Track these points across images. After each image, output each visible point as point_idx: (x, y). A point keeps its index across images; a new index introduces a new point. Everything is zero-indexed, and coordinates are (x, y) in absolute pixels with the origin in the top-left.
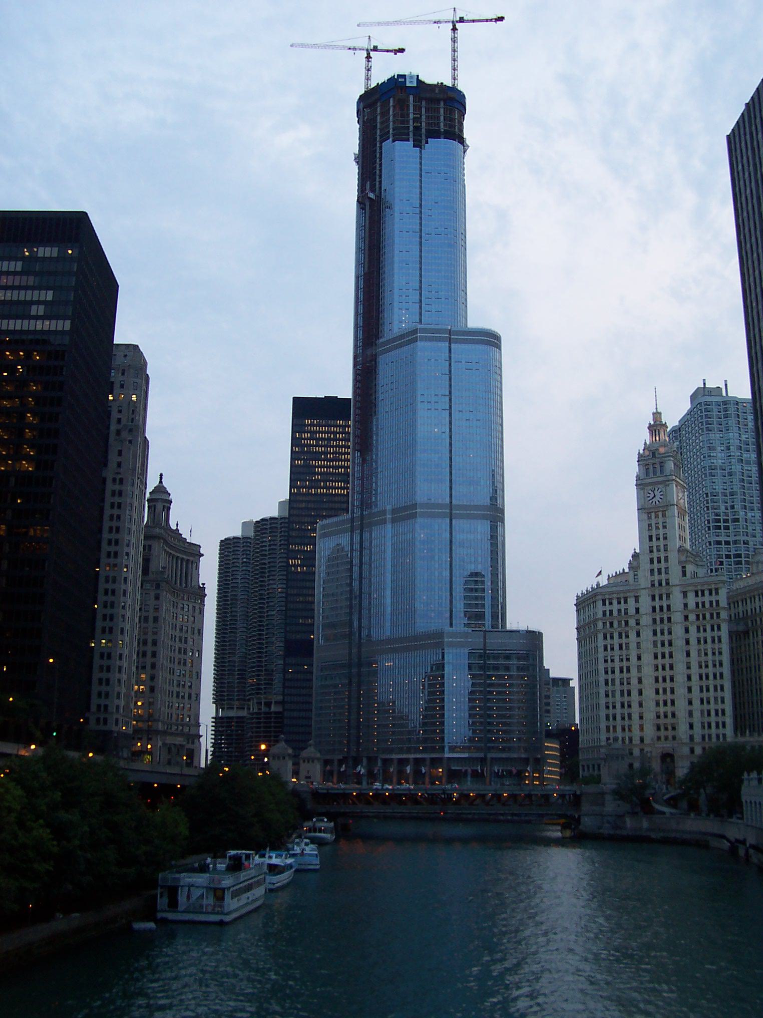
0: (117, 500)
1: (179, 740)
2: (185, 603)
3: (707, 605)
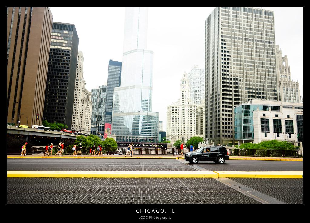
3: (192, 110)
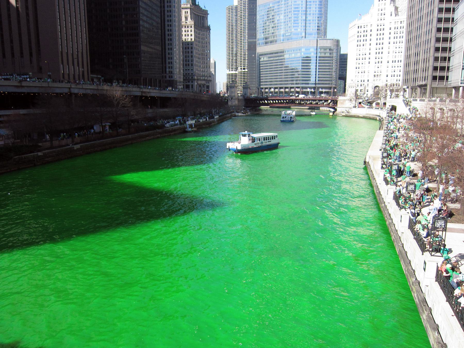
1: (203, 82)
2: (203, 33)
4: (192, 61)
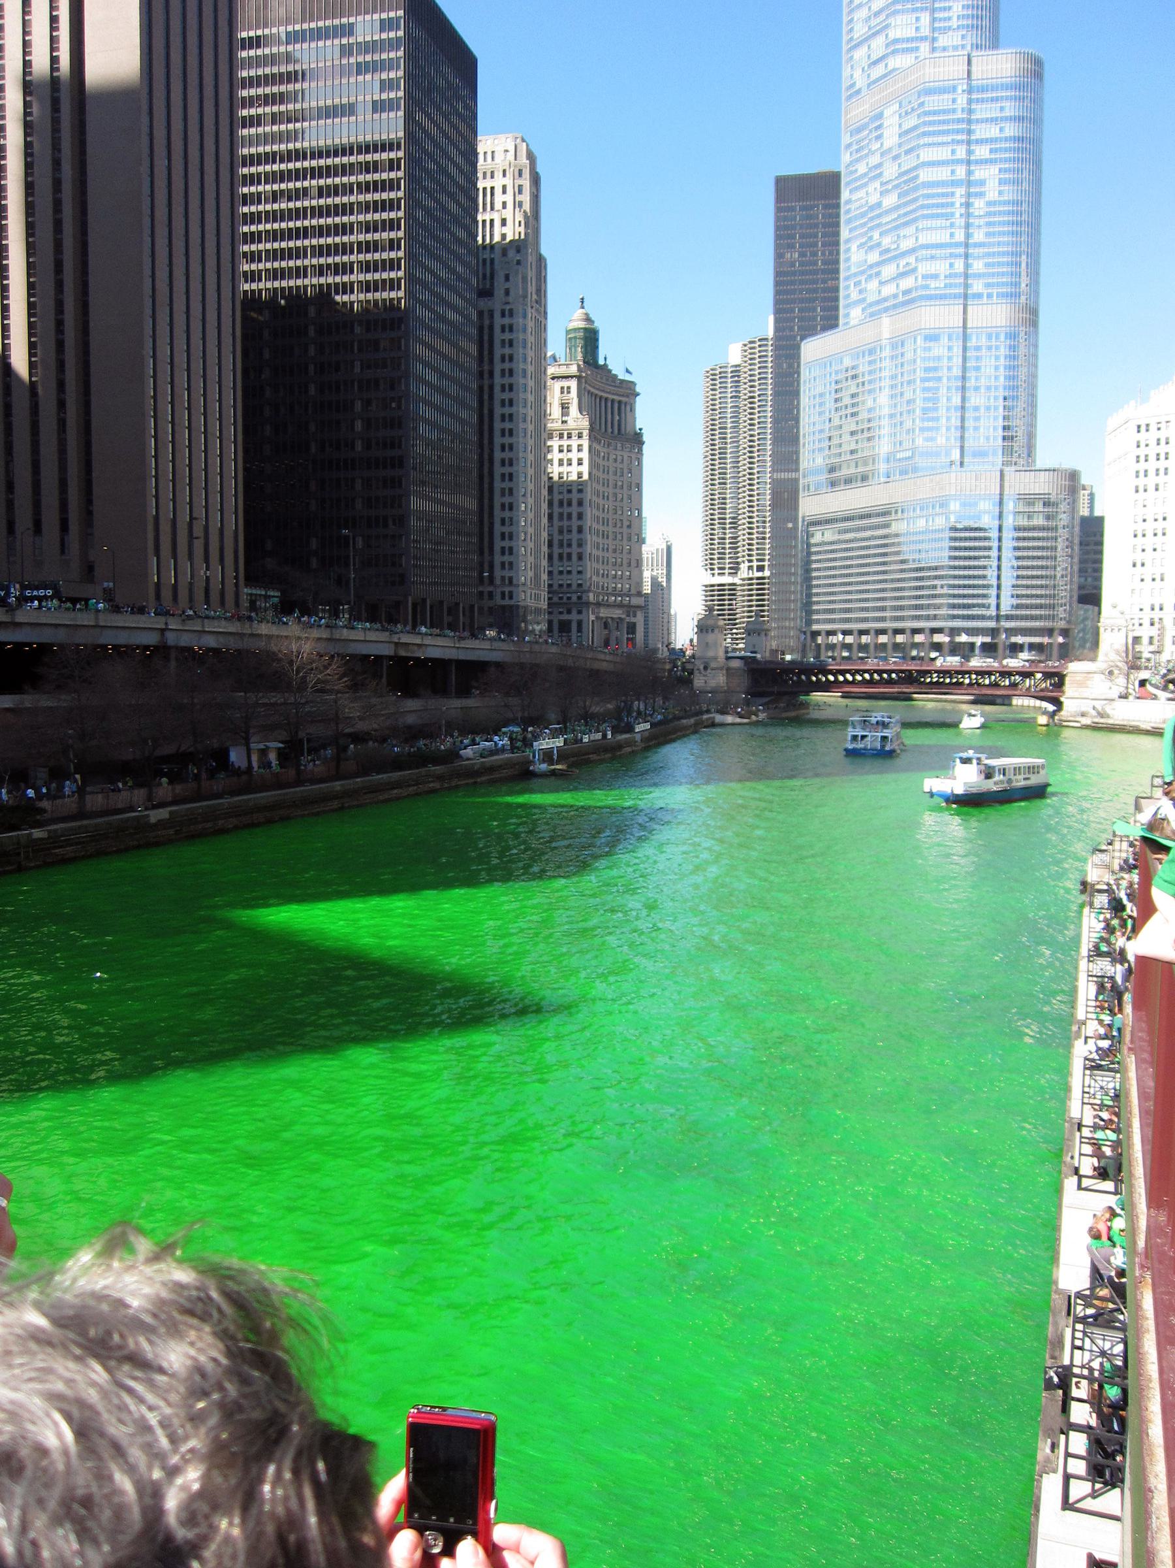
0: (507, 336)
1: (617, 613)
2: (619, 453)
4: (580, 545)
